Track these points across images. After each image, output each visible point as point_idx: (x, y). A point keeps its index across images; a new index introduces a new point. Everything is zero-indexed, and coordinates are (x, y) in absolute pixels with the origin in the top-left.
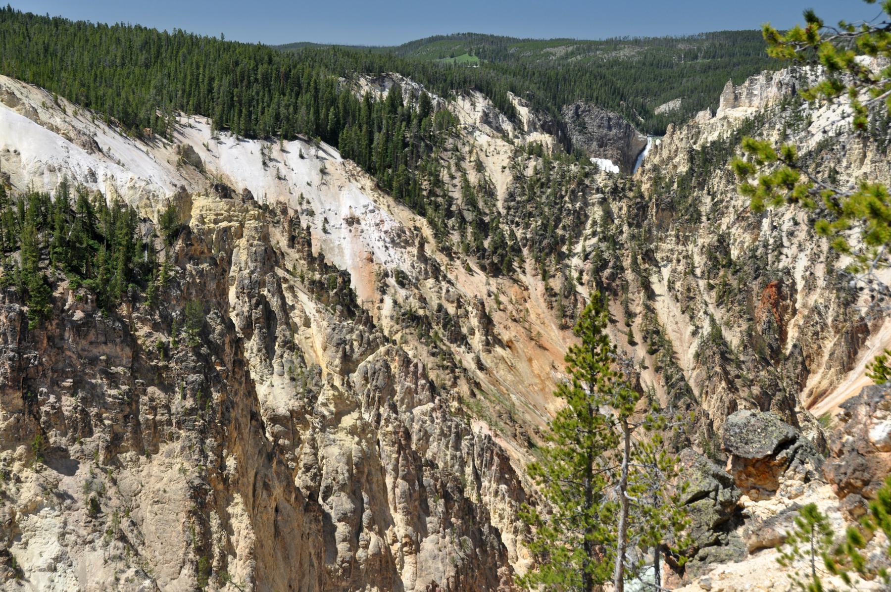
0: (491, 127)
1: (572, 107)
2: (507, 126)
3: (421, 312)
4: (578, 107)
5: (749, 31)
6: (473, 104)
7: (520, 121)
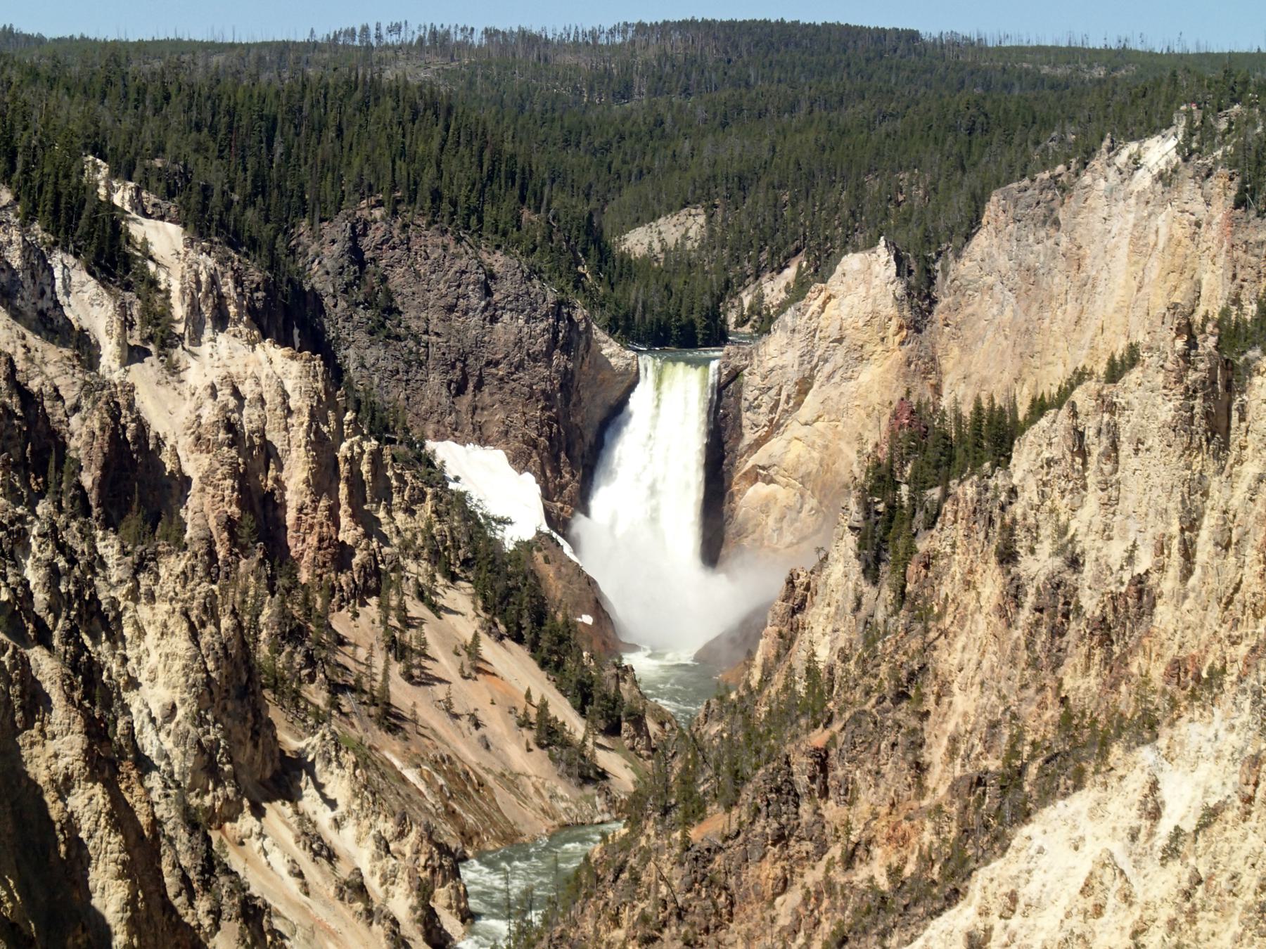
0: (16, 314)
1: (337, 230)
2: (90, 305)
4: (358, 231)
5: (766, 23)
7: (153, 283)
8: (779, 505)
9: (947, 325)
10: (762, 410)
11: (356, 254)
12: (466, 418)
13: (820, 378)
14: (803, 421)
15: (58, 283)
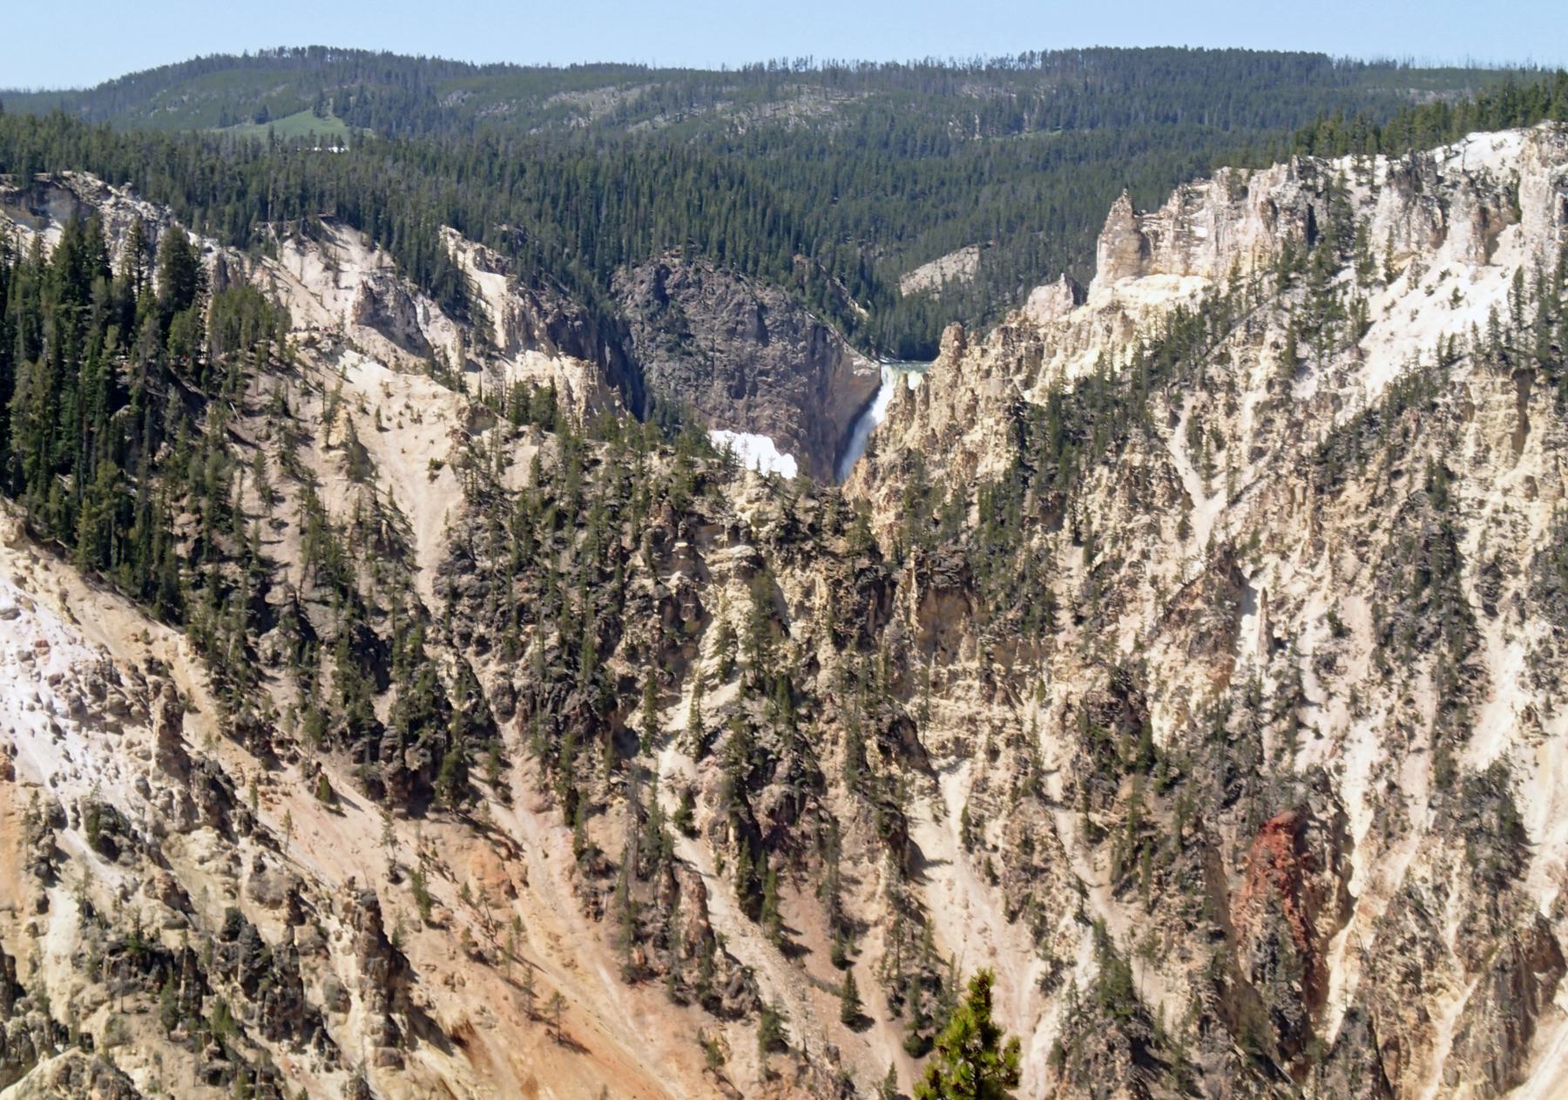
0: (391, 336)
1: (646, 273)
2: (442, 334)
3: (172, 941)
4: (662, 273)
5: (1169, 50)
6: (332, 267)
7: (483, 316)
11: (659, 291)
12: (742, 414)
15: (420, 317)
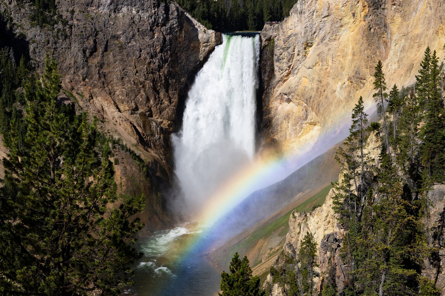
8: (294, 116)
9: (394, 5)
10: (285, 60)
12: (94, 71)
13: (317, 40)
14: (308, 67)
